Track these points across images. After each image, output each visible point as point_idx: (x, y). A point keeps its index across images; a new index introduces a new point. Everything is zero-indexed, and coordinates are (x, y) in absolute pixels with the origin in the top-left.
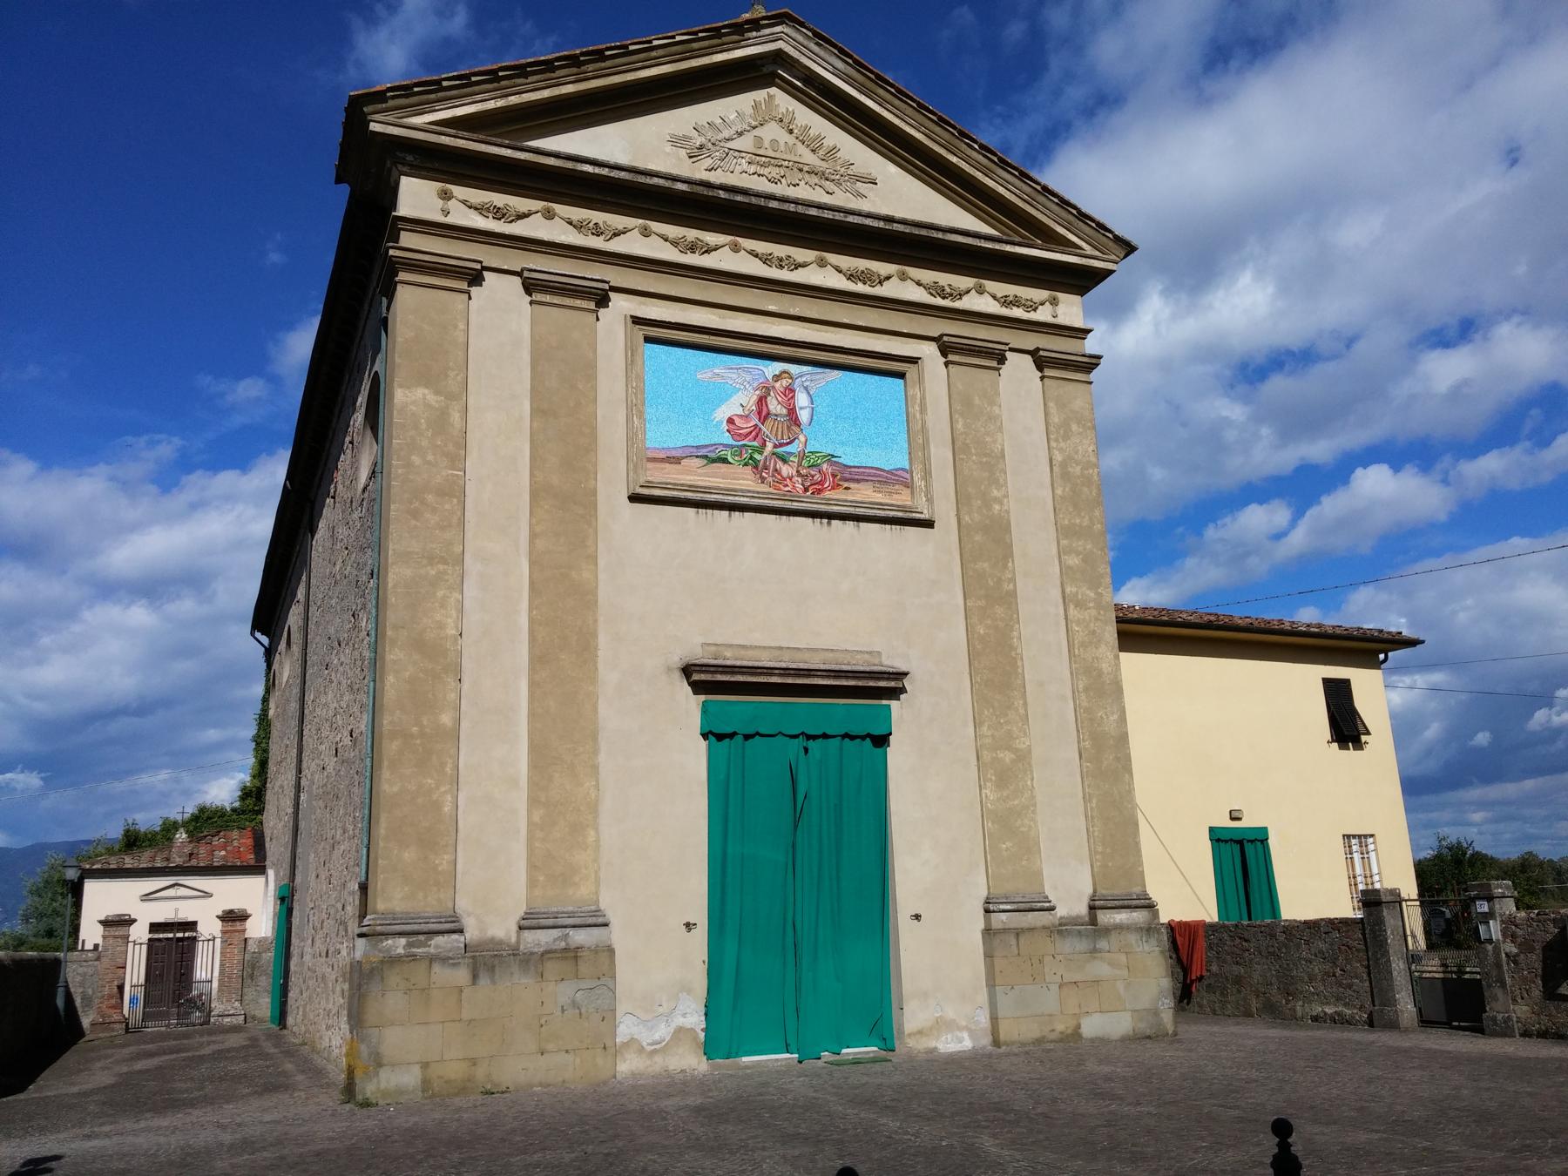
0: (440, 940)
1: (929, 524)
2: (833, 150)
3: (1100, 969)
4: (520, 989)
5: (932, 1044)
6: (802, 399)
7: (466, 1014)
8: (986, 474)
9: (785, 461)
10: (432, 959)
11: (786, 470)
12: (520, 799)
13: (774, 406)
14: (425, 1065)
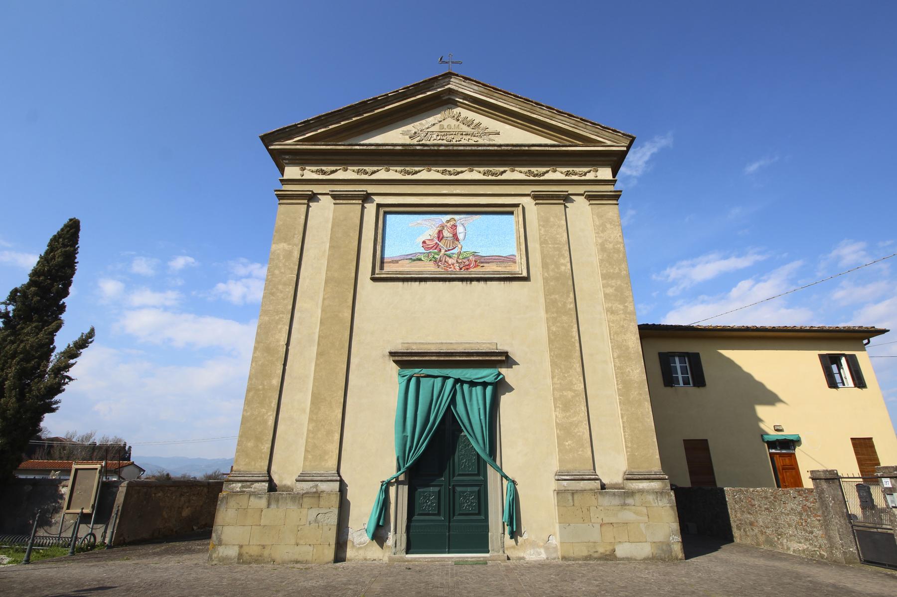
0: (256, 485)
3: (628, 515)
5: (522, 555)
6: (460, 229)
7: (263, 522)
8: (557, 253)
9: (450, 257)
10: (251, 494)
11: (450, 261)
12: (305, 418)
13: (446, 233)
14: (241, 547)
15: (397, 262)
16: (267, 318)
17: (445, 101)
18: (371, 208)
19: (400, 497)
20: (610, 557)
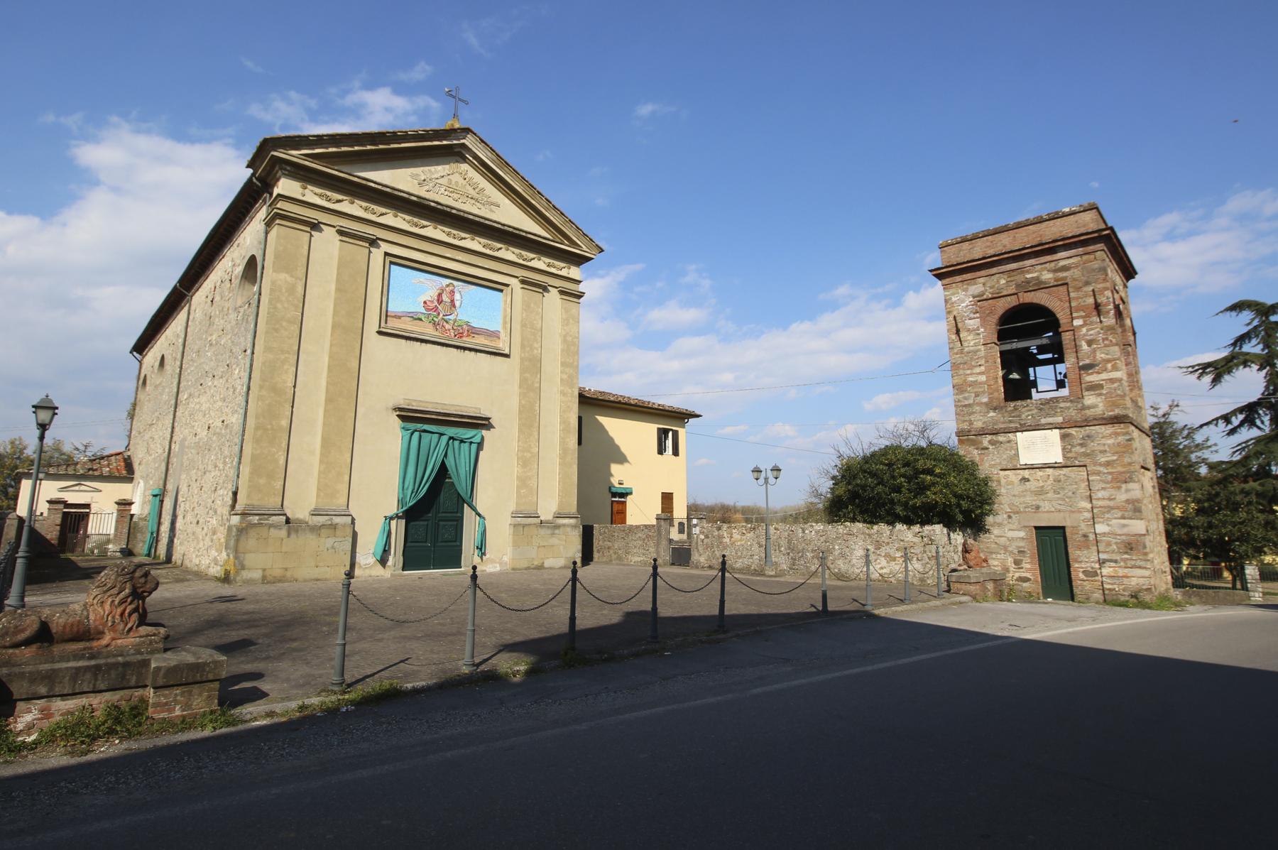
1: (507, 356)
2: (483, 190)
4: (310, 540)
6: (457, 296)
7: (284, 549)
10: (271, 526)
11: (447, 326)
13: (445, 298)
15: (400, 317)
16: (271, 356)
17: (456, 154)
18: (377, 255)
19: (398, 528)
20: (541, 567)
